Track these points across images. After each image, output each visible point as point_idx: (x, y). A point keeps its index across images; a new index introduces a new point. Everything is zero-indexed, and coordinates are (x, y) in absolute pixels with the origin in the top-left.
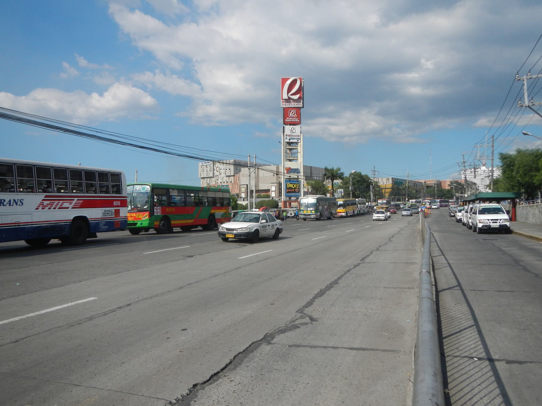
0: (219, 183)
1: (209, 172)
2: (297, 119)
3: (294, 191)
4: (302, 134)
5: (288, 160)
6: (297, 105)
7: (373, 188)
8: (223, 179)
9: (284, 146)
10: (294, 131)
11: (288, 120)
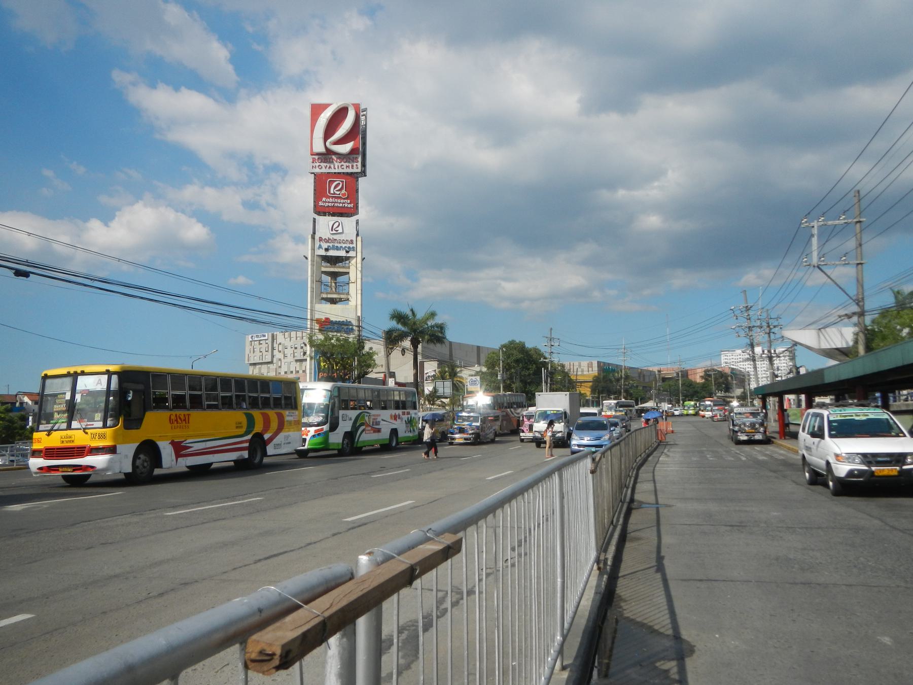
0: (283, 373)
1: (265, 353)
2: (349, 201)
4: (359, 238)
5: (323, 299)
6: (347, 167)
7: (547, 376)
8: (289, 367)
9: (312, 265)
10: (340, 230)
11: (325, 202)
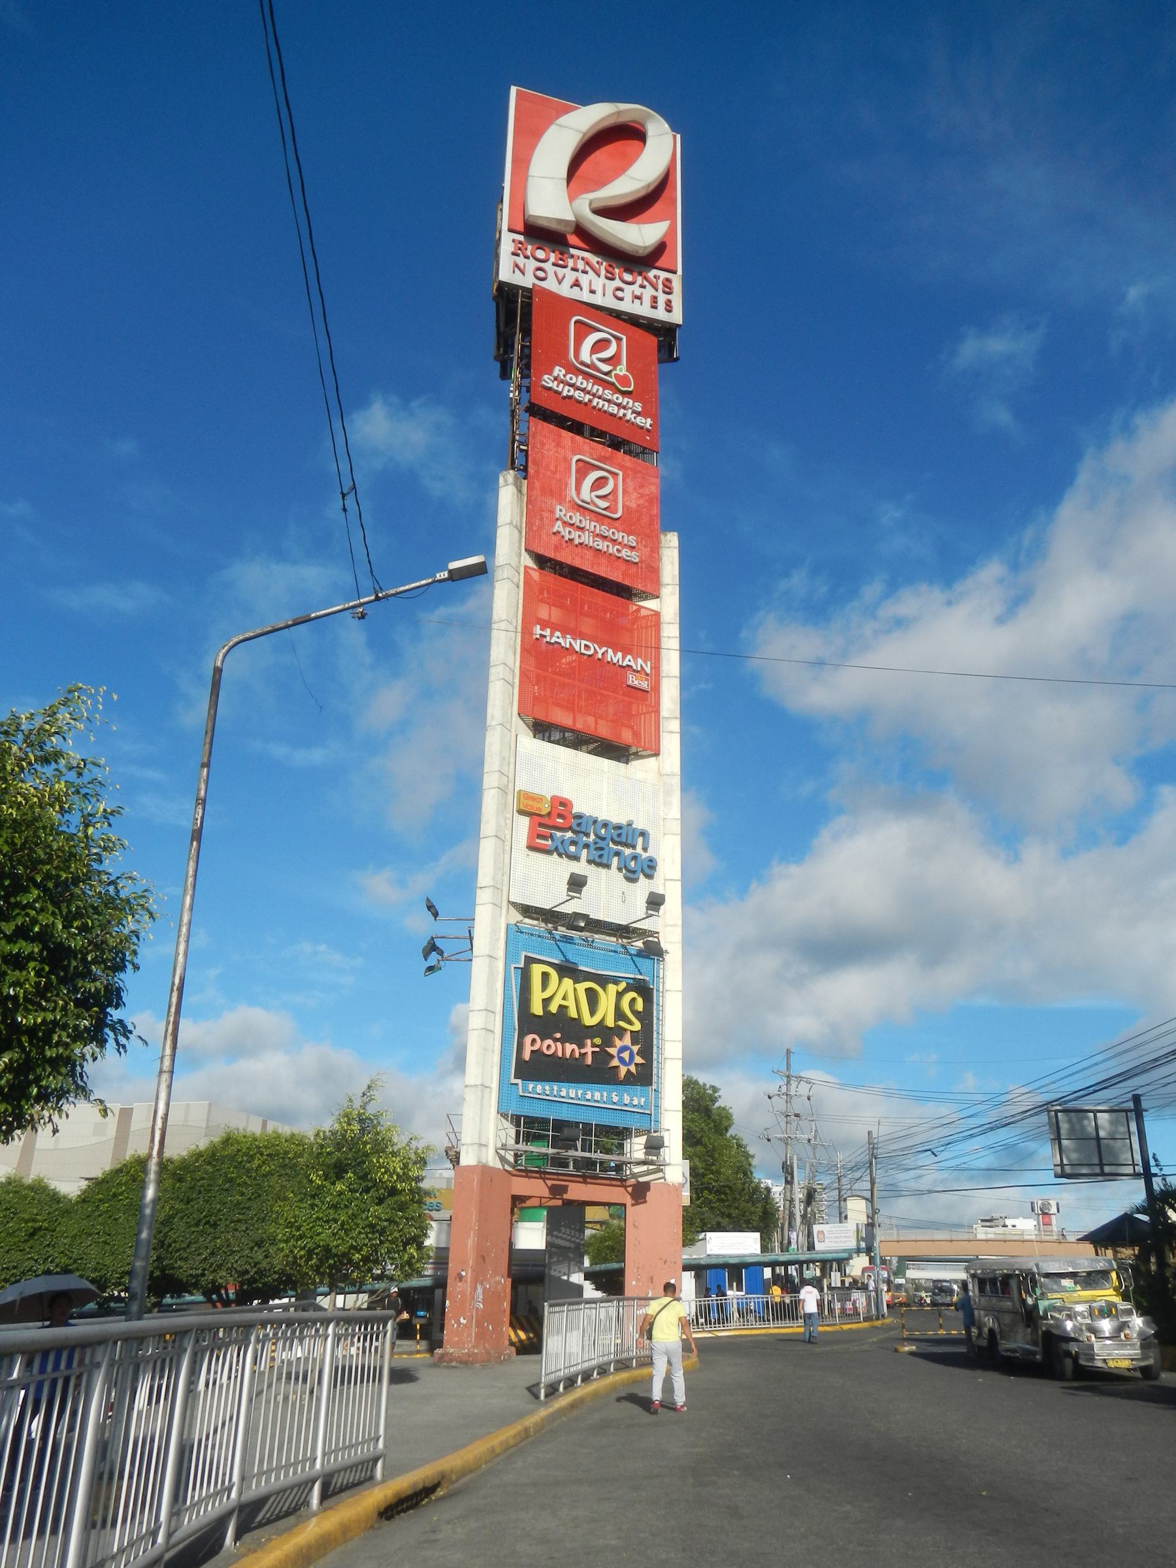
2: (638, 407)
3: (602, 1056)
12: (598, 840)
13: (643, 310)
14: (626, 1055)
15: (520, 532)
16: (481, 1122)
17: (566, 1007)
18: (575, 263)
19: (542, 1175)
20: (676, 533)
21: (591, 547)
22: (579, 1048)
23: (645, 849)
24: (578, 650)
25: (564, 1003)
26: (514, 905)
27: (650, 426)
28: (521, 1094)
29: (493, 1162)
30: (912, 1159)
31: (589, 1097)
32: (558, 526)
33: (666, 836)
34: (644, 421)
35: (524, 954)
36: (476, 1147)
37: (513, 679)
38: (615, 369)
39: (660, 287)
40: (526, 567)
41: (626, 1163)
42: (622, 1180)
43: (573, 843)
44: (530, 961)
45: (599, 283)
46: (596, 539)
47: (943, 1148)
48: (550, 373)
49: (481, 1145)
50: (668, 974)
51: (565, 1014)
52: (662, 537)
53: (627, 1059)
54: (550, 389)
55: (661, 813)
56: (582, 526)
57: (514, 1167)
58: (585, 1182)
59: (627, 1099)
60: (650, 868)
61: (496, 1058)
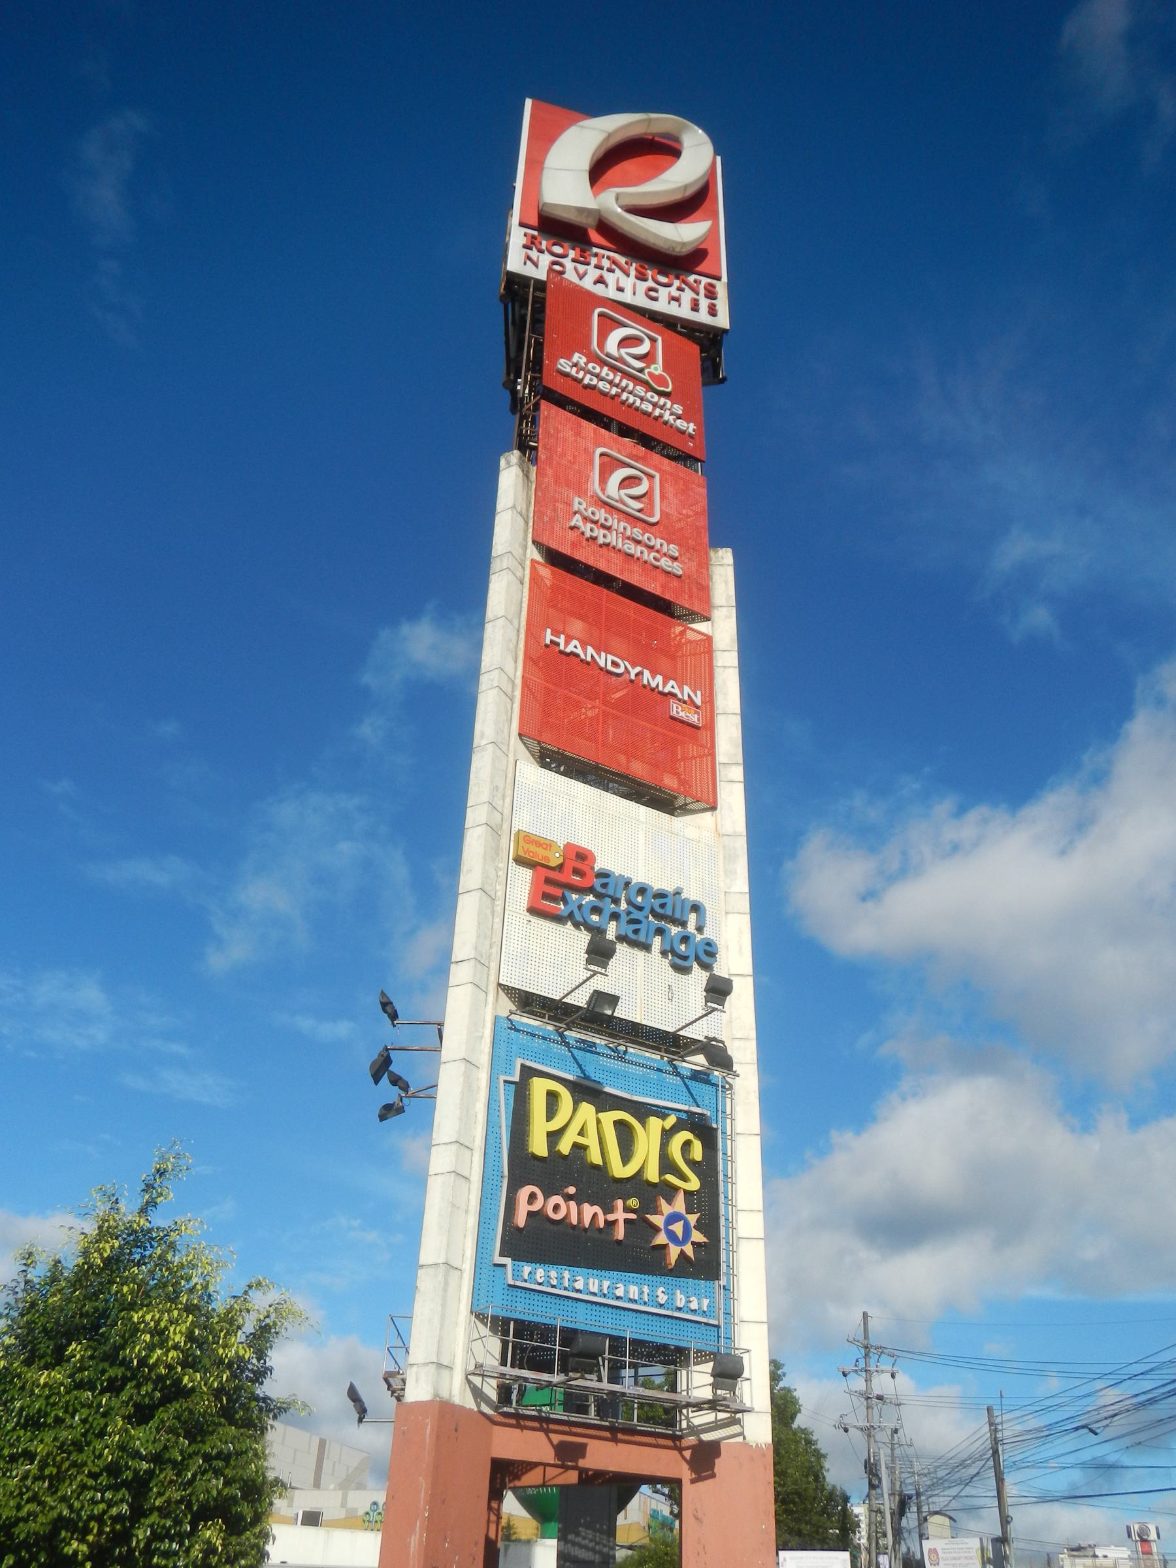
2: (678, 409)
3: (641, 1227)
12: (632, 909)
13: (683, 311)
14: (678, 1228)
15: (527, 522)
16: (442, 1325)
17: (584, 1148)
18: (599, 261)
19: (544, 1423)
20: (730, 550)
21: (620, 551)
22: (605, 1214)
23: (700, 929)
24: (602, 664)
25: (581, 1140)
26: (509, 991)
27: (694, 431)
28: (511, 1282)
29: (462, 1398)
30: (1059, 1441)
31: (620, 1292)
32: (577, 520)
33: (730, 916)
34: (685, 424)
35: (519, 1062)
36: (432, 1368)
37: (513, 691)
38: (648, 367)
39: (702, 291)
40: (533, 561)
41: (678, 1407)
42: (676, 1438)
43: (596, 910)
44: (528, 1073)
45: (628, 282)
46: (627, 541)
47: (1107, 1422)
48: (569, 358)
49: (440, 1365)
50: (739, 1109)
51: (583, 1159)
52: (712, 554)
53: (680, 1236)
54: (567, 375)
55: (722, 884)
56: (609, 524)
57: (496, 1409)
58: (615, 1440)
59: (680, 1300)
60: (707, 955)
61: (472, 1221)
